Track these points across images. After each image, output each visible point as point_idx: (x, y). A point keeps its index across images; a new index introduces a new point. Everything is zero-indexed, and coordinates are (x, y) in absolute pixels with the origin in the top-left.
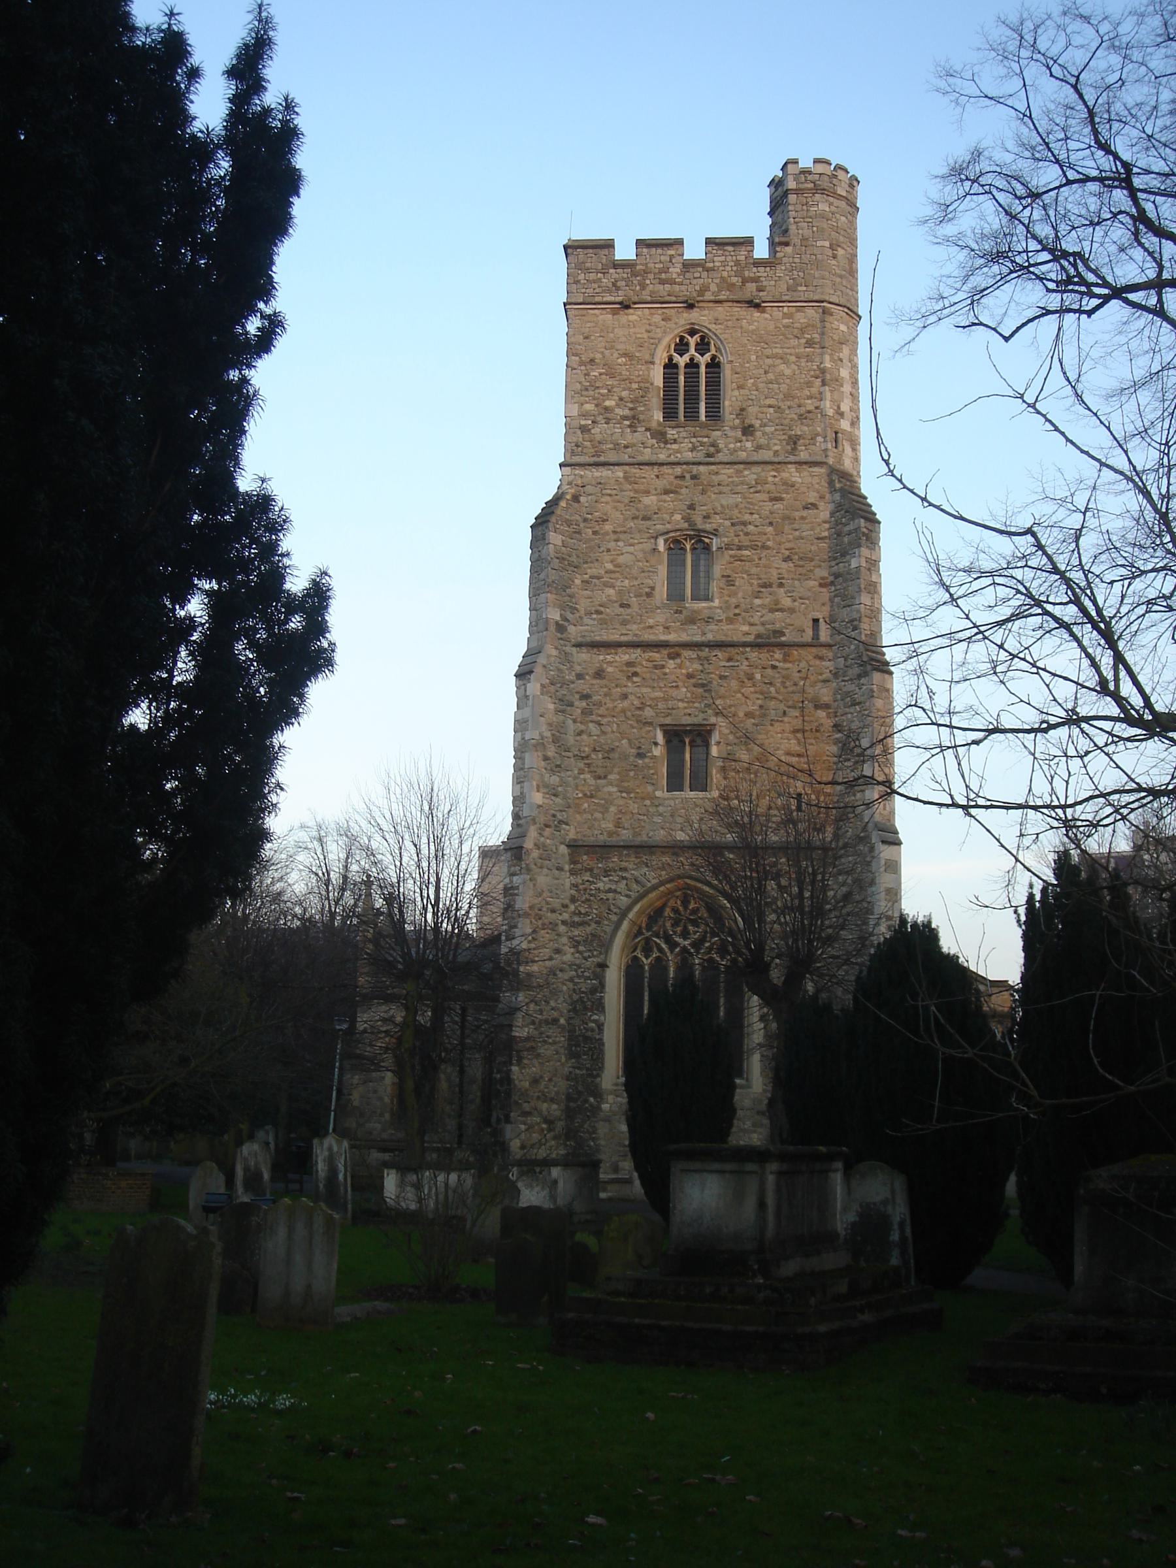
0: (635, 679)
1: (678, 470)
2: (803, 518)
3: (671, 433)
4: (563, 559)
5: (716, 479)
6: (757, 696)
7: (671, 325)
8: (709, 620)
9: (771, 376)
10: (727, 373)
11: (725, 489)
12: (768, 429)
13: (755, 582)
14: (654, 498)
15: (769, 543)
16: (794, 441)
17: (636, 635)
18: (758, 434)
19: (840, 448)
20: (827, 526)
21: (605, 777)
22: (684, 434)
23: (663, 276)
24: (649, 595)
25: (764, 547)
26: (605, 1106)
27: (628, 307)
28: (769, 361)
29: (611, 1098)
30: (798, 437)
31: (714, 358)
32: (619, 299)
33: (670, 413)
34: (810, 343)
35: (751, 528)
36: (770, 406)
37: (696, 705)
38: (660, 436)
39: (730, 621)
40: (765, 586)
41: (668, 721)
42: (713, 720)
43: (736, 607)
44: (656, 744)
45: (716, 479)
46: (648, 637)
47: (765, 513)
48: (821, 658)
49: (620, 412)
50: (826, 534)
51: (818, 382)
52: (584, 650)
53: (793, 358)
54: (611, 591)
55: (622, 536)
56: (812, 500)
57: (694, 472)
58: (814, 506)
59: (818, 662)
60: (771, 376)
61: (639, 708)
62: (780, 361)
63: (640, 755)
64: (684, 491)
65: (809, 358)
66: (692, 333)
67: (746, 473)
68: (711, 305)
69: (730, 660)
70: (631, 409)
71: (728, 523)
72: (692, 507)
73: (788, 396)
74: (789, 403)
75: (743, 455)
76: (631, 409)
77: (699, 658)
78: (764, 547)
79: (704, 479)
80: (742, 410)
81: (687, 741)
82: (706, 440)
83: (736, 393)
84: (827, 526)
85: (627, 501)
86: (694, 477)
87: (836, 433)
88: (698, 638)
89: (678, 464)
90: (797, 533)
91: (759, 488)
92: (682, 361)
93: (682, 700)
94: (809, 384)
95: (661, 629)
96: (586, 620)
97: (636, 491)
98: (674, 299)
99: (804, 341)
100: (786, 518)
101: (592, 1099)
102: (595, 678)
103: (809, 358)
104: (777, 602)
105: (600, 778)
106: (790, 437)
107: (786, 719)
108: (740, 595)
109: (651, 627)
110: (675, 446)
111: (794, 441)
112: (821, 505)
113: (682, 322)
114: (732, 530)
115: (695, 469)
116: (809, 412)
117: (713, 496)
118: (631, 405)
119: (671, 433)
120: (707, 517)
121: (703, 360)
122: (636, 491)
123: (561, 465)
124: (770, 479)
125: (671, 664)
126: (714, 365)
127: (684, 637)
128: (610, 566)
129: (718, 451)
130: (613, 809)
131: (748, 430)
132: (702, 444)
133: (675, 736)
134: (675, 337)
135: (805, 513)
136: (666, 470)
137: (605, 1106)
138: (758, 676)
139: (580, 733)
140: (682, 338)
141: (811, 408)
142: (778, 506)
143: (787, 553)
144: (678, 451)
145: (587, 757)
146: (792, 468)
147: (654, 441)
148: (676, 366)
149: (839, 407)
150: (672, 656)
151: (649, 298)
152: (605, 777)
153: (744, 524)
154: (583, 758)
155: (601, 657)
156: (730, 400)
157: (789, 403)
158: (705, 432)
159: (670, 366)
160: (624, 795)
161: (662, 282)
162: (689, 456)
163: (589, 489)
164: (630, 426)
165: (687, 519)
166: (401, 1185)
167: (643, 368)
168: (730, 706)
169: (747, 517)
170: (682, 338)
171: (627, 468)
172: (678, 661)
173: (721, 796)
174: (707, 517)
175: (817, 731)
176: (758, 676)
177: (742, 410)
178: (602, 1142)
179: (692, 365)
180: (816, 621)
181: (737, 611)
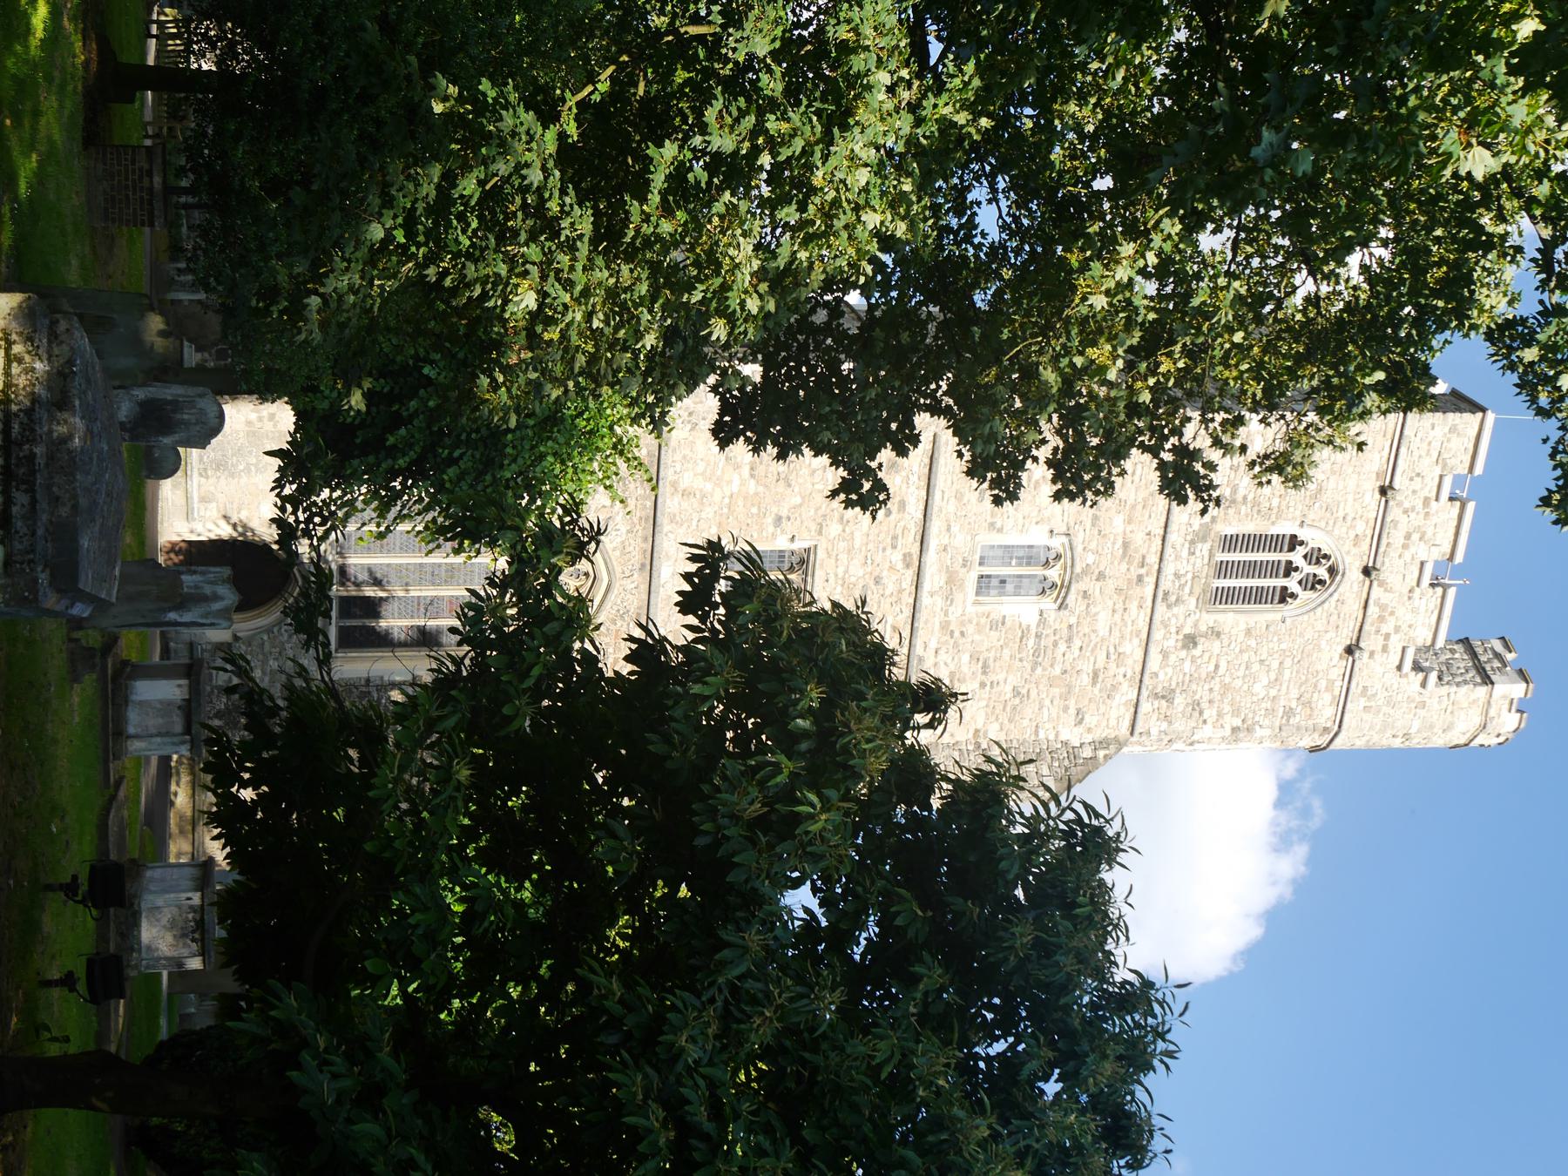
1: (1153, 559)
2: (1066, 709)
3: (1203, 549)
5: (1133, 607)
7: (1348, 545)
8: (949, 598)
9: (1256, 667)
10: (1268, 614)
11: (1117, 617)
12: (1187, 664)
13: (992, 655)
14: (1120, 530)
15: (1039, 670)
16: (1167, 696)
17: (940, 510)
18: (1183, 653)
20: (1052, 737)
21: (752, 476)
23: (1415, 537)
25: (1035, 665)
27: (1383, 491)
28: (1275, 665)
31: (1293, 596)
32: (1396, 485)
33: (1230, 543)
34: (1289, 713)
35: (1062, 647)
36: (1217, 667)
37: (839, 589)
39: (945, 626)
40: (985, 666)
41: (821, 554)
43: (962, 634)
46: (935, 526)
47: (1080, 665)
50: (1042, 735)
51: (1237, 722)
53: (1273, 693)
57: (1146, 579)
60: (1256, 667)
62: (1273, 676)
64: (1124, 566)
65: (1270, 712)
66: (1332, 571)
67: (1136, 641)
68: (1364, 596)
70: (1245, 498)
71: (1073, 620)
72: (1101, 576)
74: (1217, 688)
75: (1158, 635)
76: (1245, 498)
77: (900, 591)
78: (1035, 665)
79: (1136, 591)
80: (1218, 634)
82: (1187, 590)
83: (1243, 626)
84: (1052, 737)
86: (1140, 579)
88: (927, 586)
90: (1047, 702)
91: (1113, 657)
92: (1297, 557)
93: (846, 572)
94: (1236, 712)
95: (946, 541)
97: (1133, 507)
98: (1381, 550)
99: (1294, 705)
100: (1070, 687)
106: (1173, 691)
108: (977, 637)
109: (948, 530)
110: (1185, 553)
112: (1080, 729)
113: (1348, 560)
114: (1064, 626)
115: (1151, 580)
116: (1201, 713)
117: (1110, 603)
118: (1250, 497)
119: (1203, 549)
120: (1085, 594)
121: (1292, 584)
122: (1133, 507)
124: (1122, 670)
125: (896, 557)
129: (1169, 607)
130: (709, 487)
131: (1191, 641)
132: (1182, 587)
135: (1072, 711)
140: (1326, 557)
141: (1206, 716)
142: (1086, 679)
143: (1024, 691)
144: (1178, 558)
147: (1196, 527)
148: (1292, 549)
150: (906, 557)
151: (1388, 519)
152: (752, 476)
153: (1069, 640)
156: (1234, 619)
157: (1217, 688)
158: (1197, 590)
159: (1294, 542)
160: (727, 500)
161: (1408, 536)
162: (1169, 569)
165: (1086, 570)
166: (166, 707)
167: (1298, 513)
169: (1077, 643)
172: (900, 565)
174: (1085, 594)
177: (1218, 634)
178: (244, 479)
179: (1290, 569)
181: (957, 634)
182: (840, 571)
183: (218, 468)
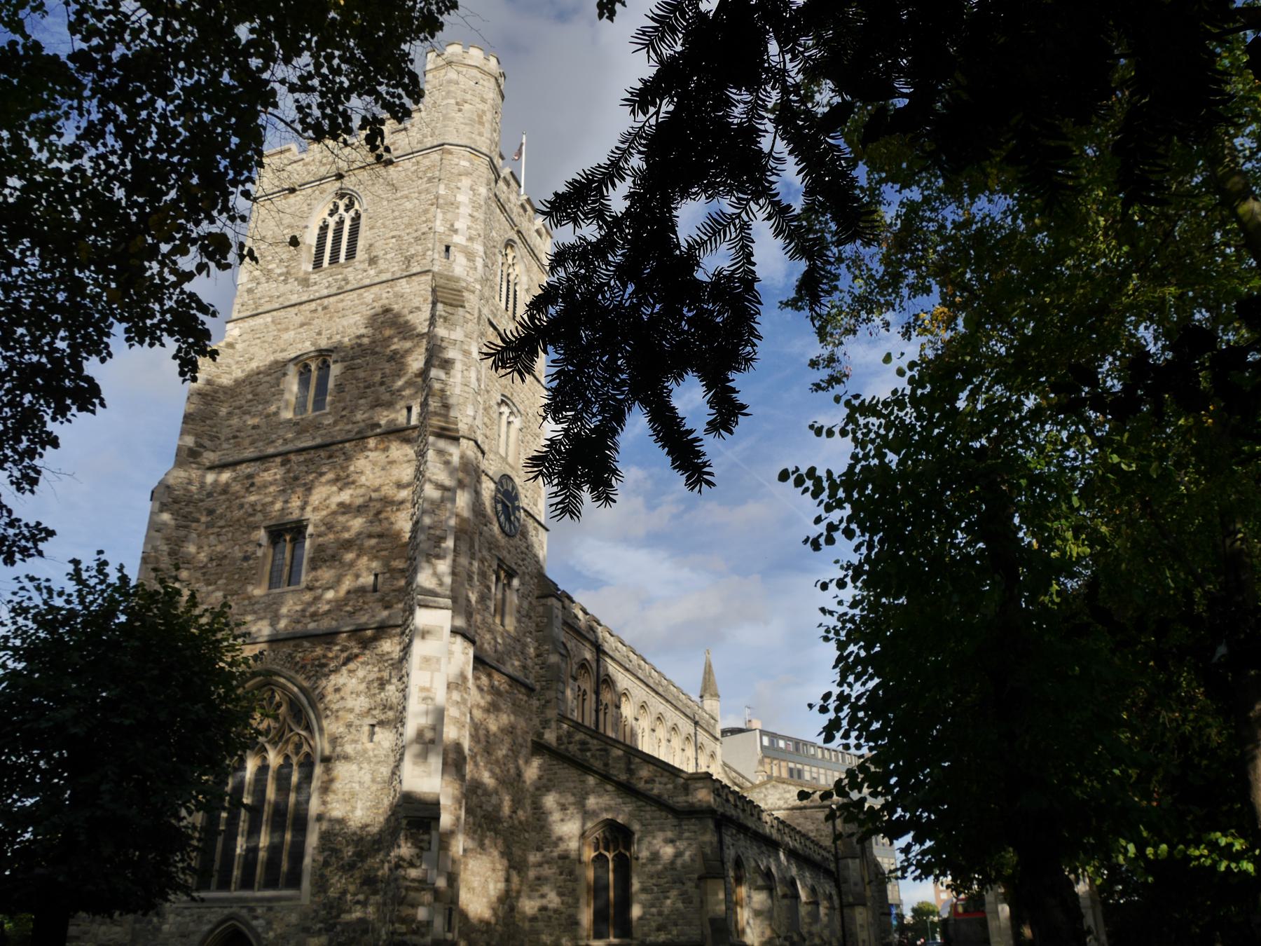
1: (313, 305)
10: (363, 221)
12: (388, 256)
18: (381, 261)
19: (452, 258)
29: (171, 918)
30: (412, 256)
33: (318, 264)
38: (305, 282)
40: (368, 387)
44: (260, 545)
45: (340, 305)
49: (278, 271)
56: (417, 305)
58: (418, 309)
63: (246, 558)
66: (342, 196)
69: (330, 457)
73: (409, 225)
81: (288, 538)
87: (448, 248)
96: (225, 446)
102: (220, 494)
104: (377, 399)
111: (408, 260)
115: (326, 301)
126: (356, 219)
128: (250, 397)
132: (336, 280)
136: (303, 307)
137: (166, 927)
149: (452, 225)
159: (324, 228)
177: (371, 245)
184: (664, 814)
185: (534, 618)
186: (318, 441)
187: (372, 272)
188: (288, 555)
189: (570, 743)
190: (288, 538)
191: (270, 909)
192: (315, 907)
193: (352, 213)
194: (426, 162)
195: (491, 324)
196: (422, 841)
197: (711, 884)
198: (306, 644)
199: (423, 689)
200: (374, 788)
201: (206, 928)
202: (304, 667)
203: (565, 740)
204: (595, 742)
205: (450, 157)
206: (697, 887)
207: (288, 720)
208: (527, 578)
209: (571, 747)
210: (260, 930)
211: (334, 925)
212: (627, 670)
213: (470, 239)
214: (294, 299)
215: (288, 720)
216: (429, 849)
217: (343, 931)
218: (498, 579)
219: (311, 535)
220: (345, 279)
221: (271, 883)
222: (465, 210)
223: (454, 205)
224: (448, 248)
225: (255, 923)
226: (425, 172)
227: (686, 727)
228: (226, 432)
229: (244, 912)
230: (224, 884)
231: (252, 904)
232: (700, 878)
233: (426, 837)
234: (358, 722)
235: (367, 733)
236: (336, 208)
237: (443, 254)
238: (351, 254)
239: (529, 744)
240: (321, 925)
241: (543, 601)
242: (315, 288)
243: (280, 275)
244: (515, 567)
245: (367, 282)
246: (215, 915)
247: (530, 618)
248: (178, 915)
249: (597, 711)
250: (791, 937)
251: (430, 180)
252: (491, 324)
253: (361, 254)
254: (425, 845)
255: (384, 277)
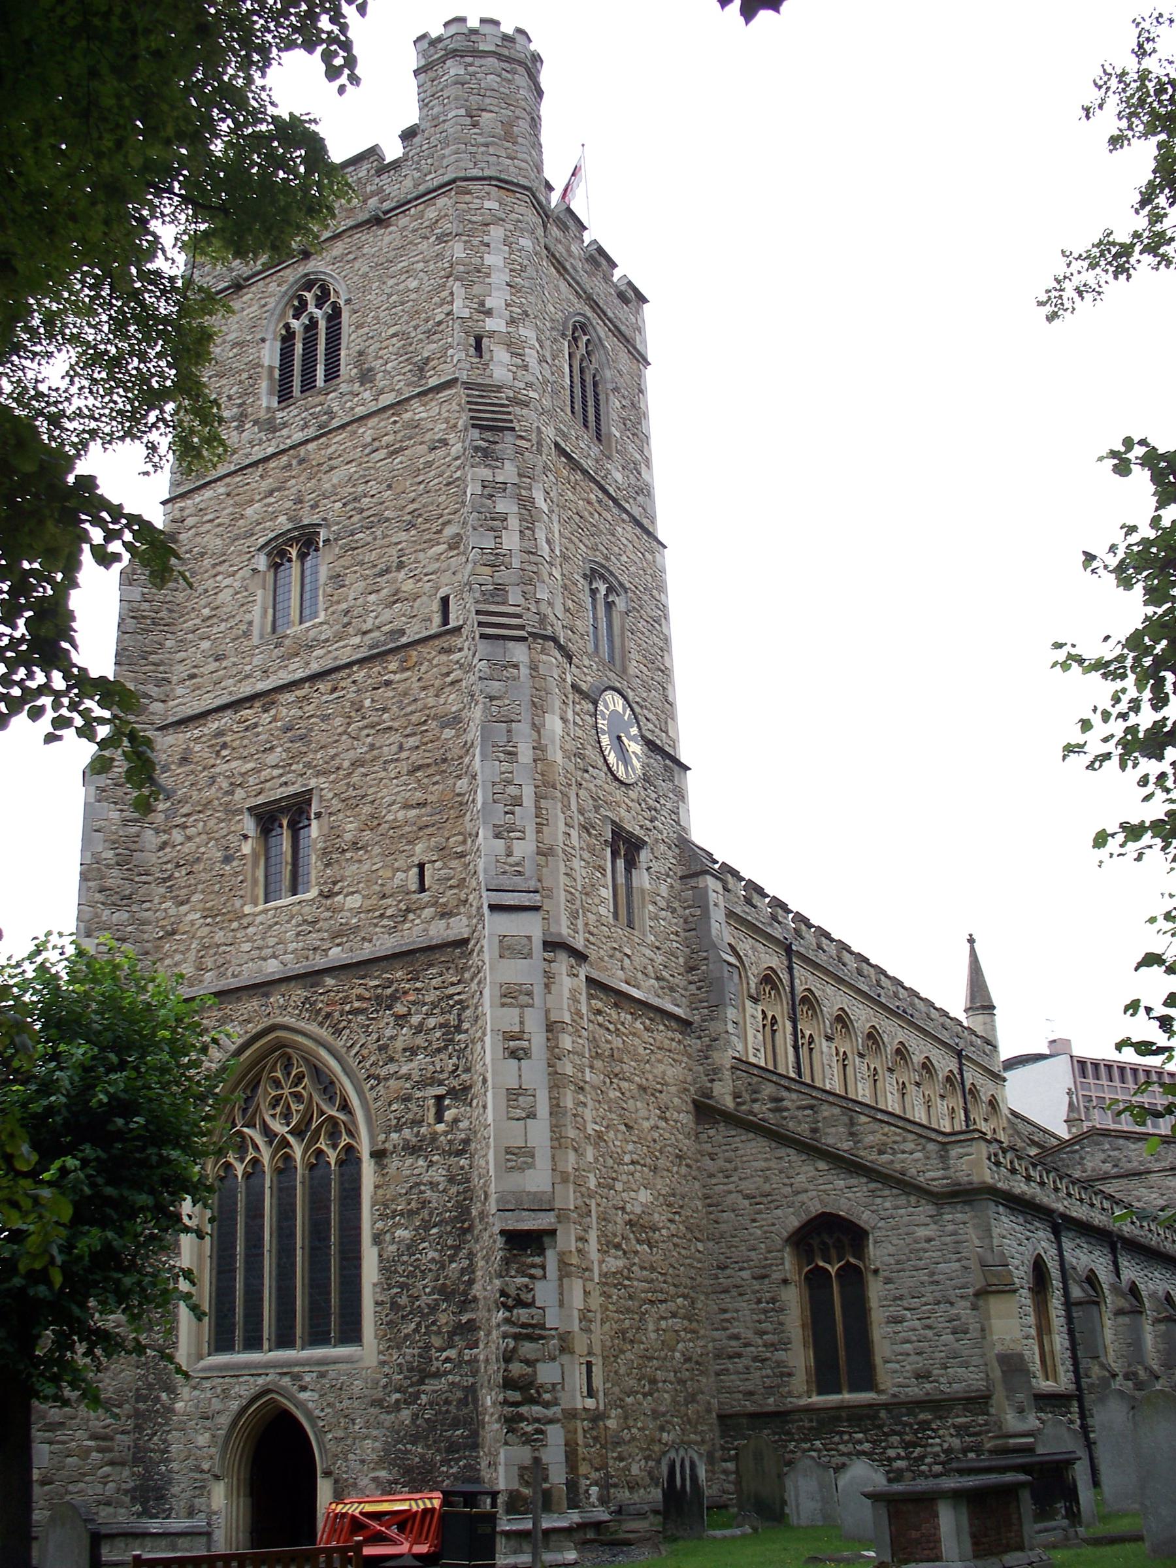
0: (224, 753)
1: (284, 459)
2: (429, 464)
4: (144, 617)
6: (366, 732)
17: (230, 693)
19: (486, 356)
22: (295, 412)
24: (247, 634)
26: (179, 1405)
33: (284, 395)
37: (294, 767)
38: (271, 427)
42: (313, 783)
44: (246, 837)
48: (449, 651)
52: (171, 730)
53: (421, 265)
54: (205, 645)
55: (219, 569)
59: (444, 658)
61: (227, 793)
63: (227, 860)
66: (308, 286)
67: (361, 430)
69: (334, 690)
81: (285, 823)
85: (227, 521)
87: (479, 340)
89: (284, 451)
91: (376, 444)
96: (180, 691)
101: (164, 1396)
102: (180, 765)
103: (439, 256)
105: (182, 904)
107: (404, 755)
111: (421, 369)
112: (452, 438)
115: (302, 451)
116: (440, 323)
120: (315, 506)
123: (164, 503)
125: (266, 718)
127: (284, 677)
128: (206, 612)
133: (267, 818)
134: (291, 299)
136: (272, 464)
137: (179, 1405)
138: (367, 703)
139: (164, 845)
145: (170, 878)
146: (415, 404)
149: (482, 304)
154: (165, 880)
155: (189, 735)
159: (288, 337)
160: (209, 920)
163: (190, 521)
164: (237, 428)
168: (333, 758)
170: (301, 299)
171: (228, 480)
173: (321, 894)
174: (315, 506)
175: (445, 760)
176: (367, 703)
178: (174, 1466)
179: (313, 324)
180: (445, 601)
181: (346, 620)
182: (276, 772)
183: (163, 1497)
184: (913, 1199)
185: (680, 911)
186: (315, 667)
187: (367, 395)
188: (286, 845)
189: (755, 1101)
190: (285, 823)
191: (322, 1375)
192: (386, 1370)
193: (327, 308)
194: (431, 213)
195: (562, 452)
196: (534, 1266)
197: (996, 1305)
198: (330, 981)
199: (509, 1037)
200: (453, 1190)
201: (235, 1406)
202: (328, 1015)
203: (746, 1097)
204: (794, 1096)
205: (467, 198)
206: (974, 1308)
207: (316, 1098)
208: (662, 847)
209: (756, 1106)
210: (310, 1405)
211: (417, 1395)
212: (840, 980)
213: (512, 321)
214: (258, 453)
215: (316, 1098)
216: (545, 1277)
217: (431, 1403)
218: (615, 854)
219: (318, 815)
220: (331, 414)
221: (318, 1337)
222: (500, 278)
223: (481, 272)
224: (479, 340)
225: (303, 1396)
226: (432, 227)
227: (945, 1064)
228: (180, 671)
229: (286, 1381)
230: (253, 1343)
231: (296, 1369)
232: (977, 1294)
233: (537, 1260)
234: (419, 1094)
235: (433, 1110)
236: (303, 304)
237: (472, 351)
238: (332, 373)
239: (691, 1107)
240: (398, 1396)
241: (692, 882)
242: (285, 432)
243: (233, 419)
244: (638, 832)
245: (360, 411)
246: (244, 1389)
247: (674, 911)
248: (195, 1388)
249: (796, 1048)
250: (1135, 1374)
251: (441, 239)
252: (562, 452)
253: (346, 369)
254: (537, 1272)
255: (387, 399)
